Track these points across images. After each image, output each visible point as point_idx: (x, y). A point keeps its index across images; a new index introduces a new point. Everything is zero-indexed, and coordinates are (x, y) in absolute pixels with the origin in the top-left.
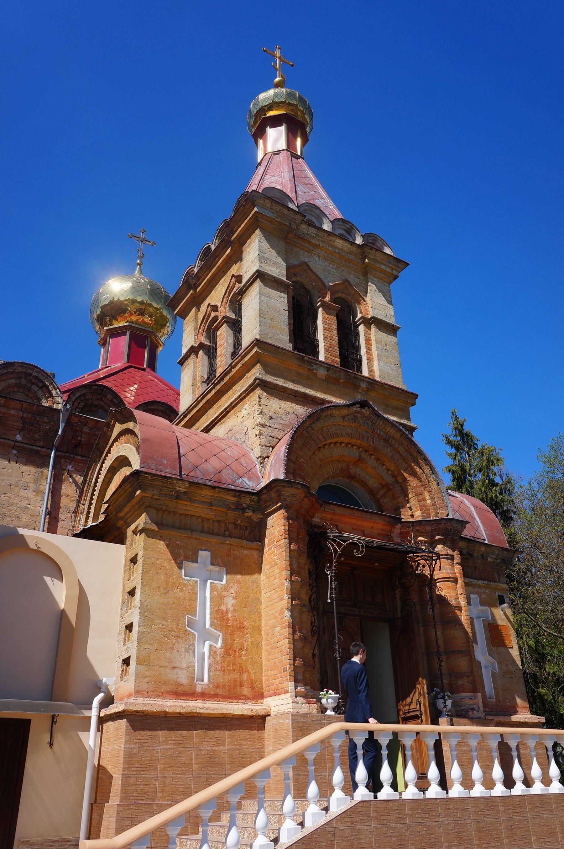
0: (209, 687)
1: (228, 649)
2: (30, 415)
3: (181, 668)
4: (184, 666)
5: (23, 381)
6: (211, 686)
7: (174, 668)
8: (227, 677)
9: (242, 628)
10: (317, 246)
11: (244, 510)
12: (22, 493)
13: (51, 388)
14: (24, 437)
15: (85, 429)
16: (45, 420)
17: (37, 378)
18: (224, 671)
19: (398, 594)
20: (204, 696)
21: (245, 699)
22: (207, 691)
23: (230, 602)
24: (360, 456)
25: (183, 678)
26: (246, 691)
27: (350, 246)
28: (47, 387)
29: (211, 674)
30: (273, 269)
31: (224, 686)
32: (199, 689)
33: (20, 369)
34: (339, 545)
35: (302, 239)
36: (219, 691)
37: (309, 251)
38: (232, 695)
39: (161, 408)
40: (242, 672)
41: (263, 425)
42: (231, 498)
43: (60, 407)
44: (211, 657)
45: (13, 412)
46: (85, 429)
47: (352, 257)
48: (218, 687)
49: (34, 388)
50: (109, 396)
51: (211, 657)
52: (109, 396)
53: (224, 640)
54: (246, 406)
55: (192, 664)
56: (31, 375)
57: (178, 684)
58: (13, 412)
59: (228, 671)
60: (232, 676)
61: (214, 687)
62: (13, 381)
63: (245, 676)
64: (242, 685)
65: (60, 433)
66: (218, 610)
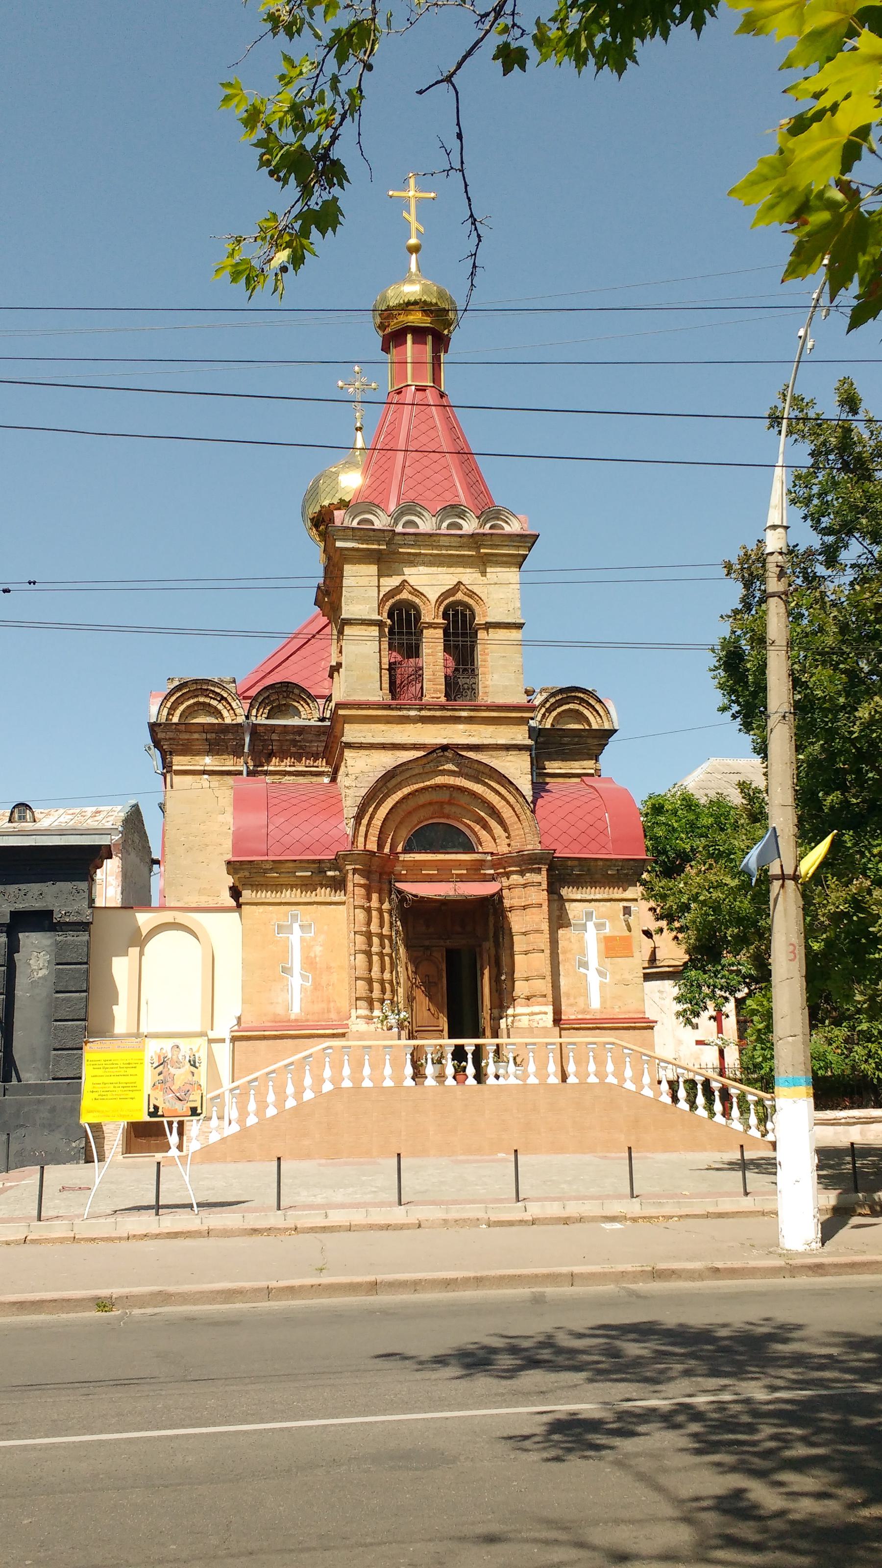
1: (316, 986)
2: (214, 735)
11: (325, 872)
12: (221, 818)
15: (275, 737)
16: (230, 736)
17: (213, 692)
19: (491, 920)
23: (318, 949)
24: (451, 795)
27: (459, 539)
28: (226, 699)
30: (361, 607)
31: (313, 1014)
33: (194, 687)
40: (329, 1002)
45: (196, 736)
46: (275, 737)
49: (214, 703)
50: (296, 691)
52: (296, 691)
53: (314, 979)
56: (207, 690)
58: (196, 736)
62: (191, 701)
63: (332, 1005)
64: (329, 1011)
66: (307, 957)
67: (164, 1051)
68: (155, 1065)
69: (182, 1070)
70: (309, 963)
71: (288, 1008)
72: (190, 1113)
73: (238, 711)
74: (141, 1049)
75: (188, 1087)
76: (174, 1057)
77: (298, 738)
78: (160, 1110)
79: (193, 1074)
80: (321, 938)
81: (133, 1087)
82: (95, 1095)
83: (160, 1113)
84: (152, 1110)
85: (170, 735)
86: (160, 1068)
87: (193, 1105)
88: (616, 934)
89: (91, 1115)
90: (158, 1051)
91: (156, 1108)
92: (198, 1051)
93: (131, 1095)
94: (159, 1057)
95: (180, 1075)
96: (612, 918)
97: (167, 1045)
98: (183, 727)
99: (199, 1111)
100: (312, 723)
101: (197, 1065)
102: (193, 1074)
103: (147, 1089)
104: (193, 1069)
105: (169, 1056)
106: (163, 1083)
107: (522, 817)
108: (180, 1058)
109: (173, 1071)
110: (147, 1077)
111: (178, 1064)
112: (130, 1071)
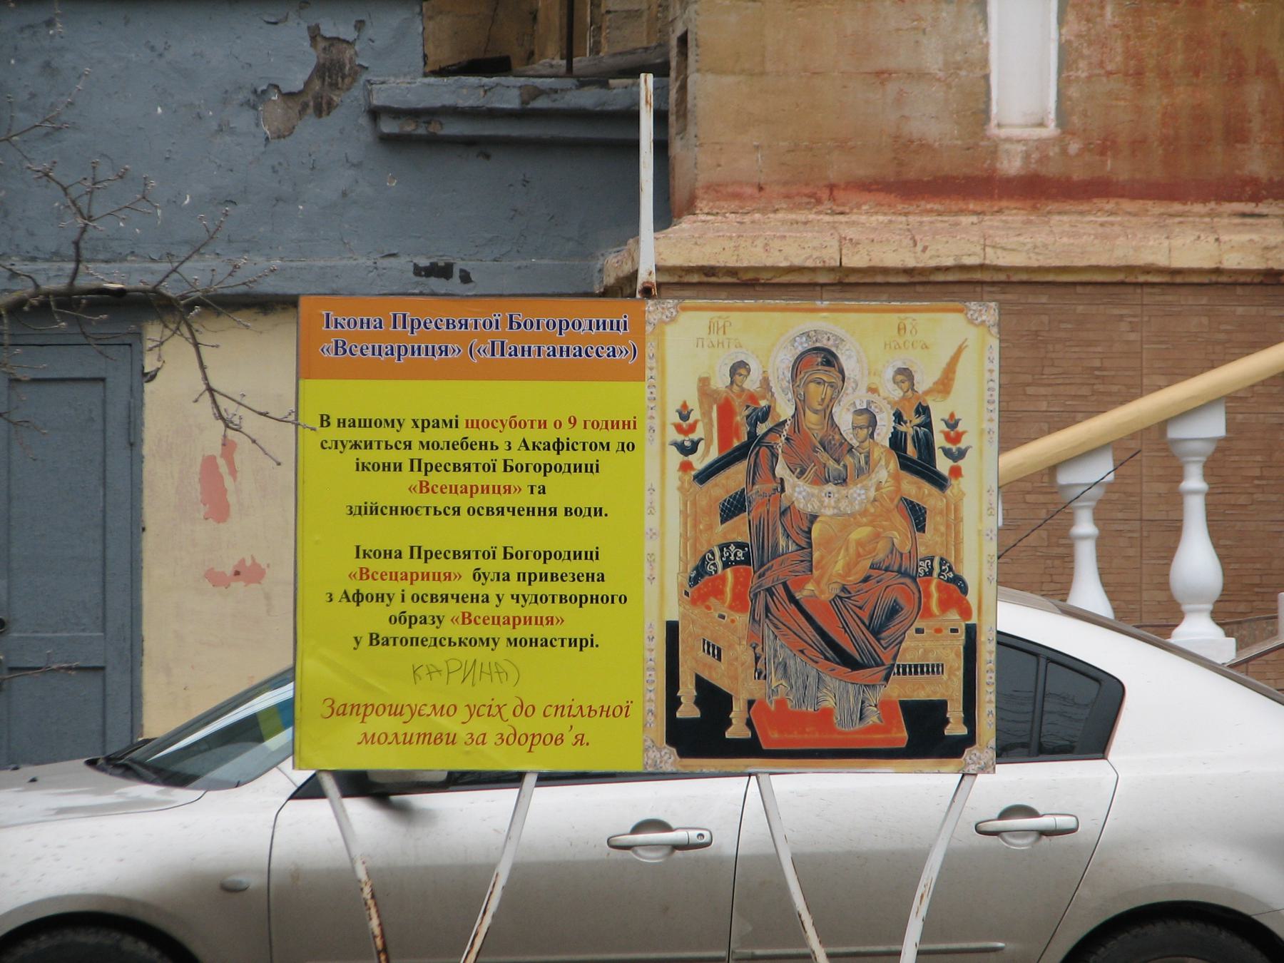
0: (1064, 151)
3: (919, 75)
4: (933, 61)
6: (1074, 147)
7: (882, 76)
8: (1155, 102)
18: (1139, 73)
20: (1038, 189)
21: (1256, 198)
22: (1052, 170)
25: (930, 120)
29: (1073, 92)
31: (1138, 144)
32: (1012, 165)
36: (1118, 168)
40: (1238, 76)
44: (1071, 17)
48: (1107, 146)
51: (1071, 17)
55: (975, 53)
57: (905, 146)
59: (1164, 74)
60: (1183, 95)
61: (1086, 148)
63: (1255, 92)
64: (1236, 134)
67: (752, 383)
68: (700, 461)
69: (858, 495)
71: (976, 105)
72: (901, 735)
74: (630, 365)
75: (893, 590)
76: (812, 420)
78: (738, 713)
79: (917, 516)
81: (582, 579)
82: (375, 617)
83: (737, 730)
84: (688, 710)
86: (735, 477)
87: (922, 690)
89: (353, 727)
90: (720, 382)
91: (714, 700)
92: (945, 385)
93: (576, 621)
94: (726, 411)
95: (846, 516)
97: (765, 341)
99: (955, 728)
101: (943, 465)
102: (917, 516)
103: (662, 597)
104: (914, 488)
105: (785, 410)
106: (749, 559)
108: (844, 419)
109: (800, 493)
110: (650, 525)
111: (830, 457)
112: (562, 489)
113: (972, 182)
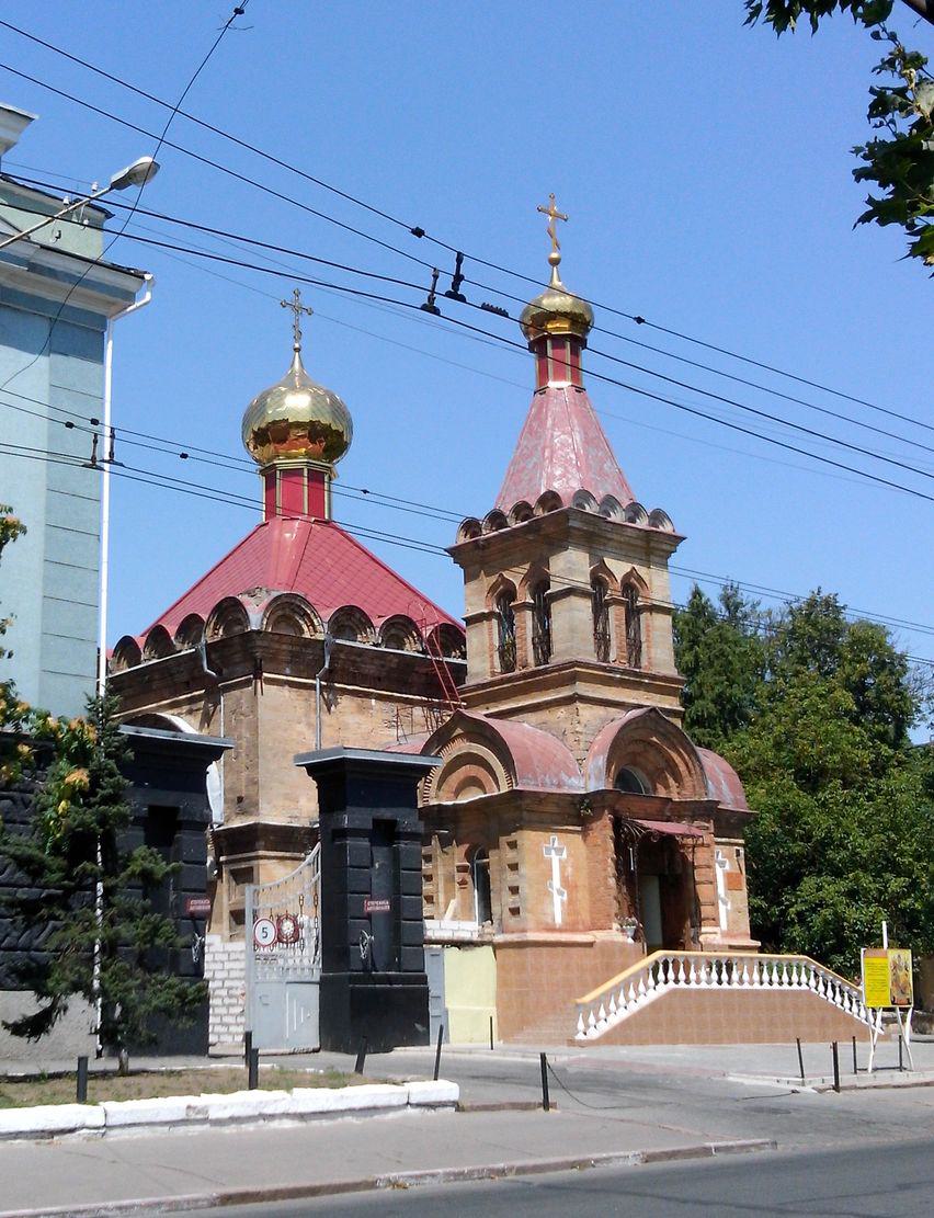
1: (571, 901)
2: (298, 648)
5: (288, 611)
9: (576, 886)
10: (610, 539)
13: (312, 615)
14: (292, 670)
15: (342, 656)
20: (560, 930)
23: (570, 870)
25: (550, 921)
26: (581, 927)
34: (640, 832)
35: (599, 536)
37: (605, 545)
38: (572, 928)
39: (401, 621)
41: (581, 733)
42: (569, 798)
43: (321, 637)
45: (284, 647)
47: (639, 543)
50: (358, 615)
52: (358, 615)
54: (562, 710)
57: (547, 924)
62: (280, 613)
65: (326, 666)
70: (565, 881)
73: (319, 628)
77: (359, 659)
80: (572, 860)
85: (265, 644)
88: (733, 871)
96: (730, 858)
98: (277, 637)
100: (367, 646)
107: (693, 772)
113: (552, 929)
